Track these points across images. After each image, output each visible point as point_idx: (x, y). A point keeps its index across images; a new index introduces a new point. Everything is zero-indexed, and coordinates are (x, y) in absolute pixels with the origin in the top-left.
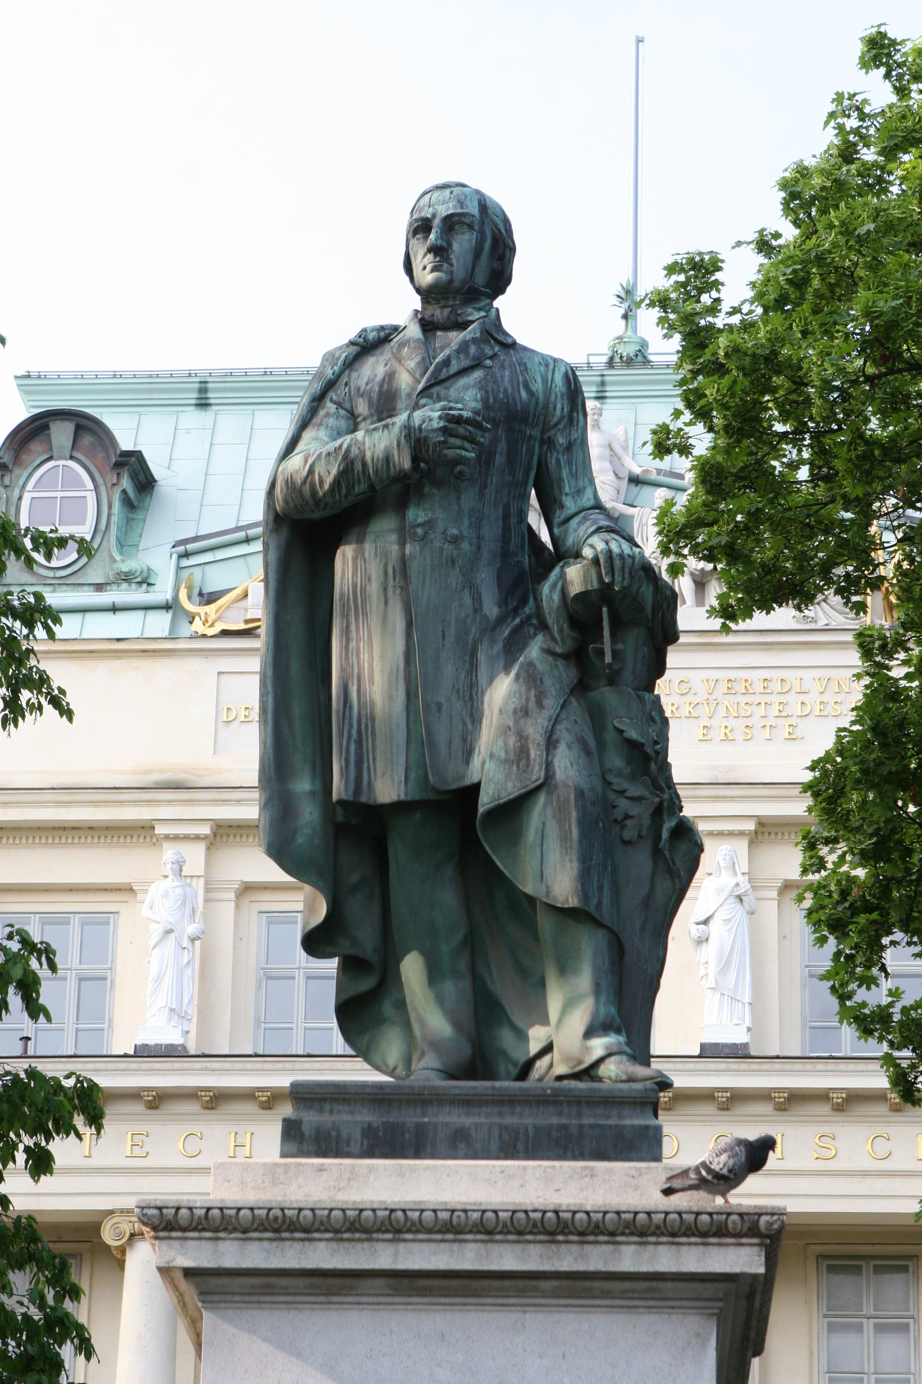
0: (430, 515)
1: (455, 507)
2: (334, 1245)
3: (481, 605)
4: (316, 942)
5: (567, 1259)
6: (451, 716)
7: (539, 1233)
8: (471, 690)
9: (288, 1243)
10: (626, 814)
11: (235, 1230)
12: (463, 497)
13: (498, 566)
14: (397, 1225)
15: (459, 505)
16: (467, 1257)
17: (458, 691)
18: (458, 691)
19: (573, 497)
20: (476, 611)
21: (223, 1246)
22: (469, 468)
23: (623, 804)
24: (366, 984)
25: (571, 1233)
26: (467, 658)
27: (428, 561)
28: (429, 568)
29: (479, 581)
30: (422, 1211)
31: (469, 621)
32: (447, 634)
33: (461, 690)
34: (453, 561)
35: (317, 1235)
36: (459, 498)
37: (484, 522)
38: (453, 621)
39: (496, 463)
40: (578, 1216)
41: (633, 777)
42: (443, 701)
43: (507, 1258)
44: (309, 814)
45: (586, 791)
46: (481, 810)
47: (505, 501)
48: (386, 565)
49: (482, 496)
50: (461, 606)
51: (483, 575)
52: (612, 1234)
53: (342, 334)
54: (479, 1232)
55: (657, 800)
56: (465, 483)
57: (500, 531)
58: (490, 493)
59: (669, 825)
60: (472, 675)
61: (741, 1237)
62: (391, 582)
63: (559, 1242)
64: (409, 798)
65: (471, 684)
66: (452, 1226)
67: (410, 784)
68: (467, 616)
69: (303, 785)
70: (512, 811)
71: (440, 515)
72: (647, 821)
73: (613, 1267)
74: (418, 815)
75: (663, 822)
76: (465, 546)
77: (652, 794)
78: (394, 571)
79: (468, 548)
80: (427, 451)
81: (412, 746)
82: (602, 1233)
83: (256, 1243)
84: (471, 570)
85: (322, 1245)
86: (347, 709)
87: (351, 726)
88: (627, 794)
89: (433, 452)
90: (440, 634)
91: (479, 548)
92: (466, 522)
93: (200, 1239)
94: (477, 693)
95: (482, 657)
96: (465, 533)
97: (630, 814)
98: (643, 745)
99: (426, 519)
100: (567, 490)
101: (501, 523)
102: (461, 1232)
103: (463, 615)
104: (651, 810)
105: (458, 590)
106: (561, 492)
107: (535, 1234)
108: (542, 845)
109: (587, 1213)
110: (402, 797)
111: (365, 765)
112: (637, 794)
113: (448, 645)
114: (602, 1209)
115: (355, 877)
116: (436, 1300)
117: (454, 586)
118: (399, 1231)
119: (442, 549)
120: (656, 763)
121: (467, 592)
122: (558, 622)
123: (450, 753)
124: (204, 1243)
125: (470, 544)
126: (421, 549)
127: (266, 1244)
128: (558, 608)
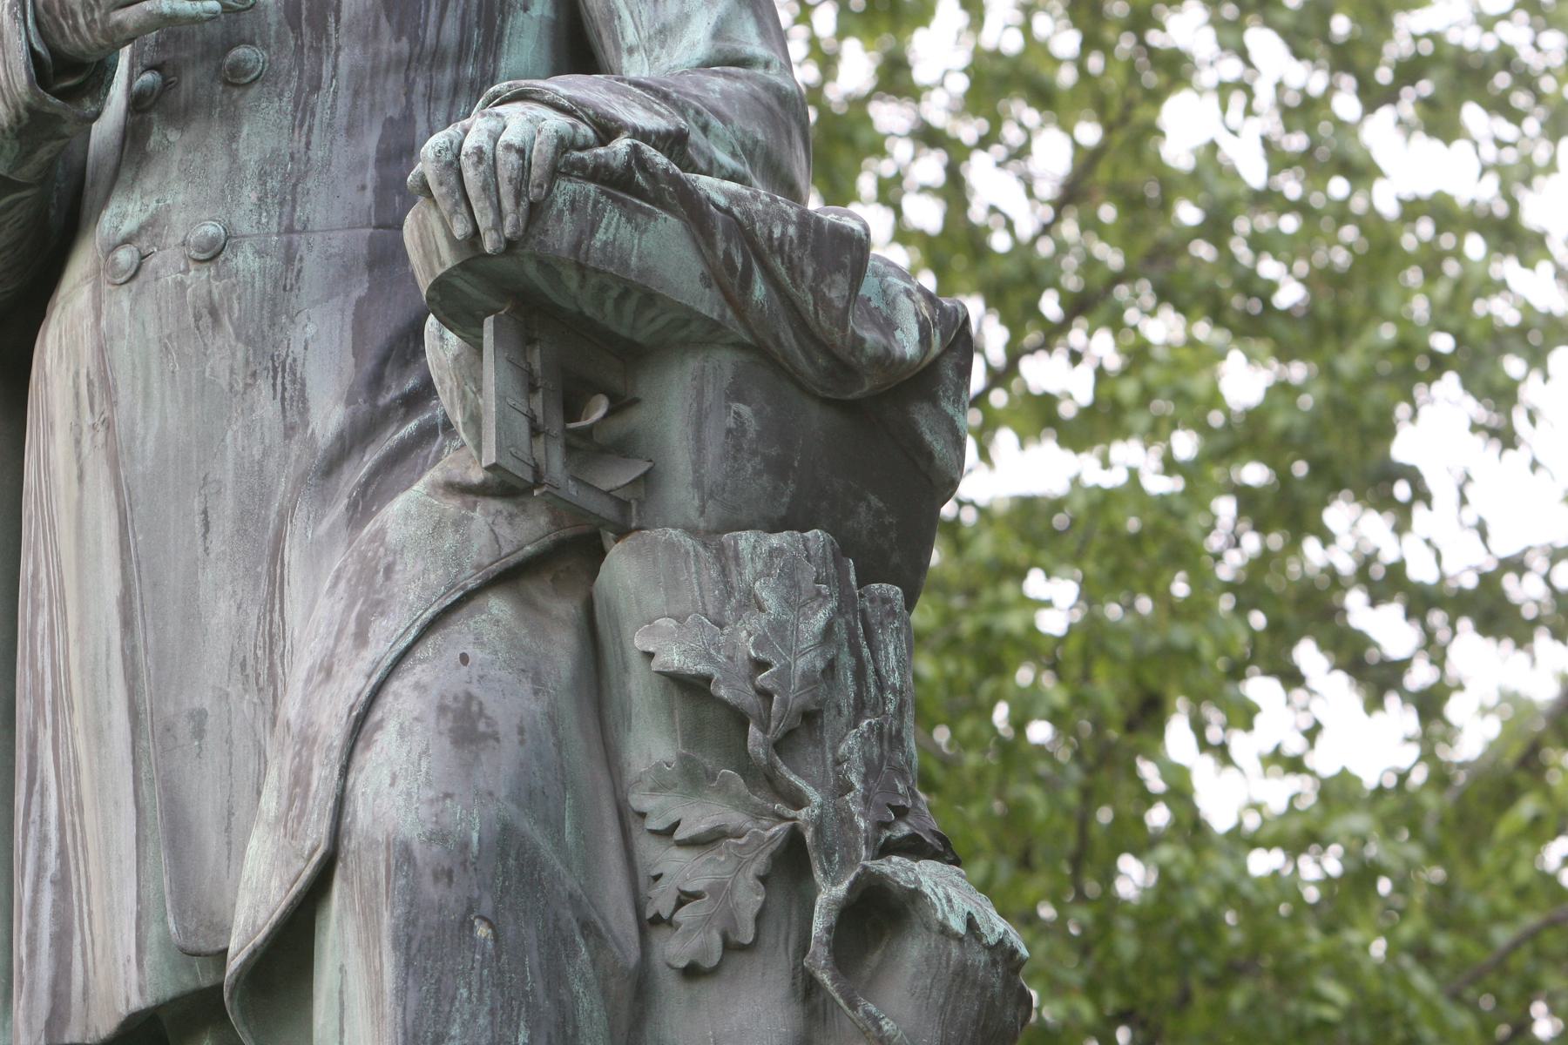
0: (153, 205)
1: (220, 164)
3: (304, 411)
6: (229, 741)
8: (271, 652)
10: (683, 892)
12: (245, 130)
13: (360, 291)
15: (233, 156)
17: (243, 665)
18: (243, 665)
19: (649, 52)
20: (289, 431)
22: (266, 47)
26: (263, 569)
27: (152, 332)
28: (155, 348)
29: (297, 348)
31: (271, 465)
32: (213, 517)
33: (250, 662)
34: (214, 313)
36: (233, 137)
37: (310, 183)
38: (230, 476)
39: (345, 16)
41: (693, 778)
42: (206, 701)
45: (416, 847)
47: (393, 112)
48: (77, 374)
49: (303, 111)
50: (249, 430)
51: (311, 330)
55: (779, 829)
56: (253, 92)
57: (369, 196)
58: (333, 102)
59: (830, 893)
60: (272, 611)
62: (87, 419)
64: (150, 1001)
65: (271, 636)
67: (148, 959)
68: (265, 454)
71: (178, 195)
72: (749, 899)
75: (815, 891)
76: (245, 261)
77: (757, 814)
78: (90, 383)
79: (255, 264)
80: (75, 29)
81: (150, 849)
84: (272, 325)
86: (36, 798)
87: (43, 840)
88: (680, 834)
89: (88, 25)
90: (198, 519)
91: (290, 257)
92: (250, 195)
94: (283, 656)
95: (293, 554)
96: (245, 227)
97: (689, 888)
98: (708, 679)
99: (144, 217)
100: (630, 36)
101: (370, 176)
103: (257, 452)
104: (759, 864)
105: (240, 387)
106: (617, 47)
108: (342, 1032)
110: (137, 1003)
111: (77, 940)
112: (703, 827)
113: (217, 544)
117: (224, 382)
119: (181, 285)
120: (764, 728)
121: (264, 386)
122: (464, 396)
123: (229, 843)
125: (260, 253)
126: (135, 301)
128: (456, 358)
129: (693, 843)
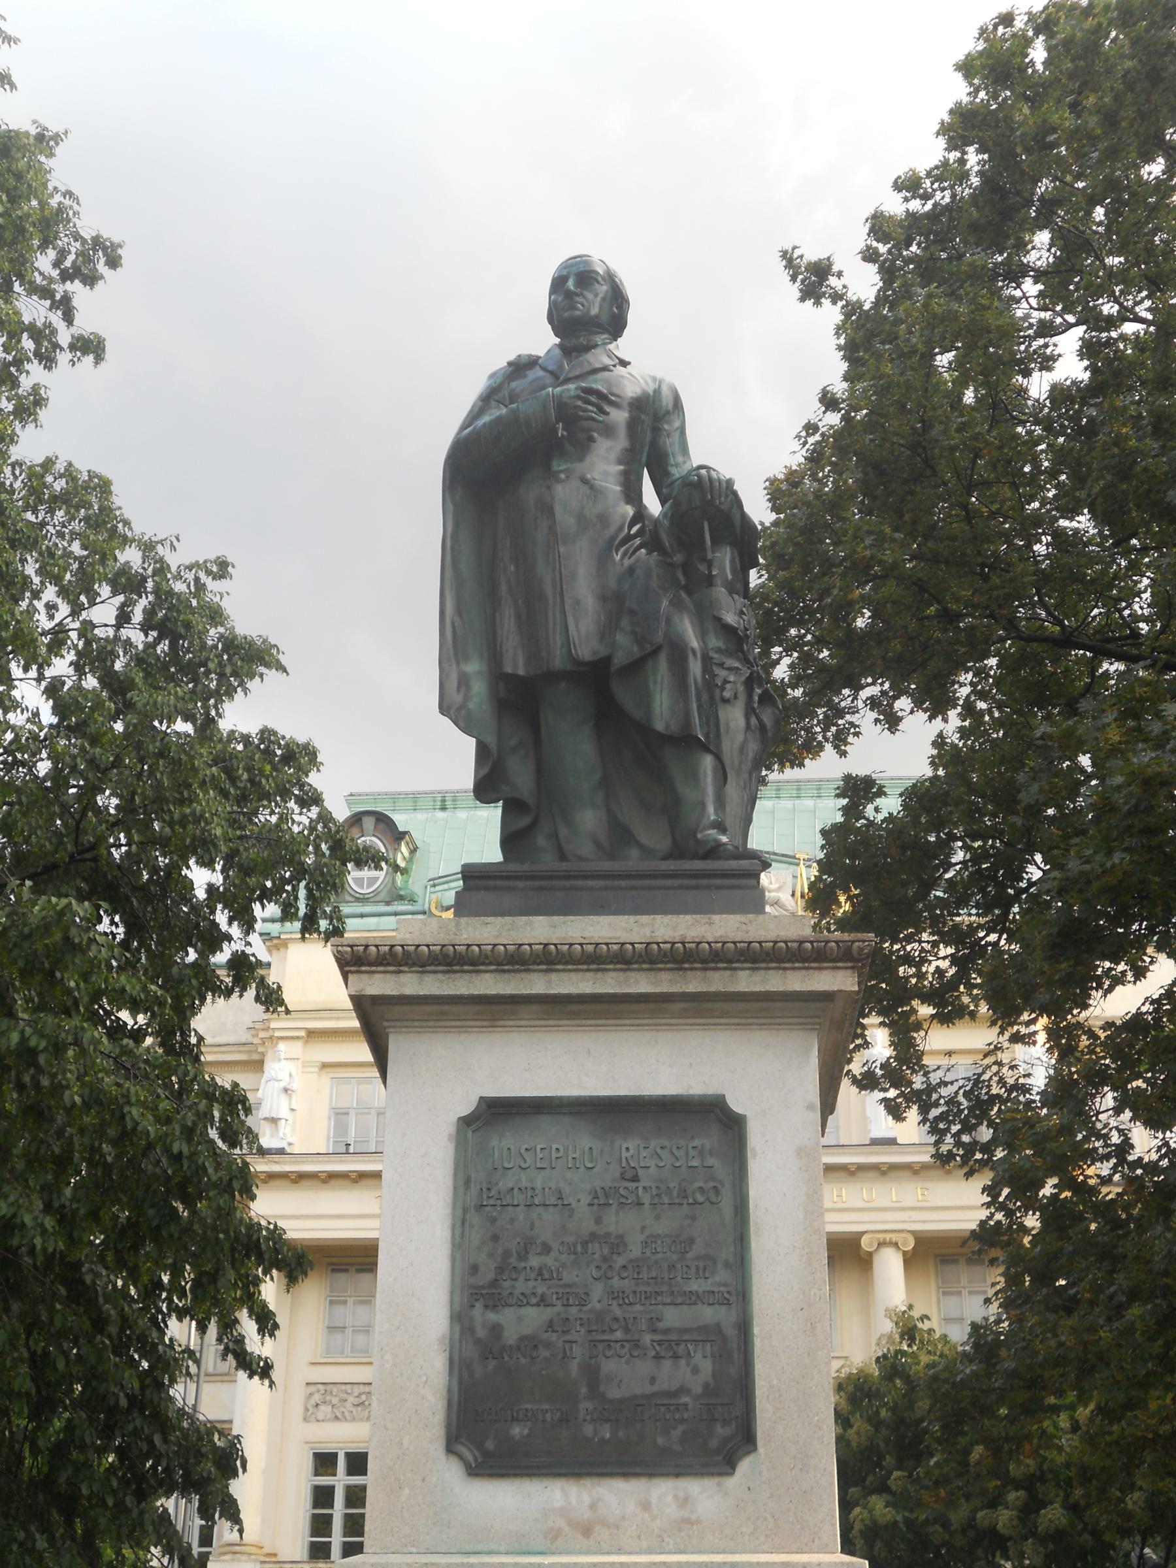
2: (498, 976)
4: (484, 791)
5: (693, 983)
7: (669, 962)
9: (457, 975)
11: (414, 964)
14: (549, 959)
16: (609, 983)
21: (404, 978)
23: (722, 673)
24: (524, 821)
25: (695, 961)
30: (571, 945)
35: (483, 968)
40: (701, 946)
43: (642, 983)
44: (479, 688)
46: (613, 668)
52: (730, 961)
53: (500, 361)
54: (619, 962)
61: (838, 961)
63: (686, 969)
66: (594, 959)
69: (473, 667)
70: (636, 668)
73: (731, 988)
74: (563, 685)
82: (721, 961)
83: (432, 976)
85: (487, 976)
93: (385, 972)
102: (604, 963)
107: (666, 963)
109: (708, 943)
114: (723, 939)
115: (514, 741)
116: (584, 1022)
118: (552, 963)
124: (388, 976)
127: (440, 976)
129: (730, 669)
